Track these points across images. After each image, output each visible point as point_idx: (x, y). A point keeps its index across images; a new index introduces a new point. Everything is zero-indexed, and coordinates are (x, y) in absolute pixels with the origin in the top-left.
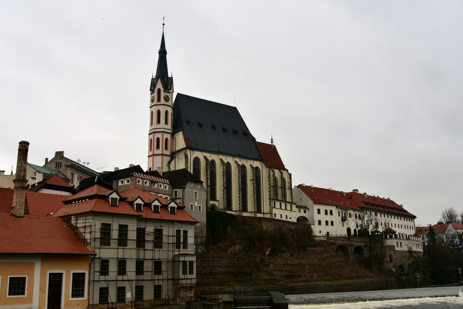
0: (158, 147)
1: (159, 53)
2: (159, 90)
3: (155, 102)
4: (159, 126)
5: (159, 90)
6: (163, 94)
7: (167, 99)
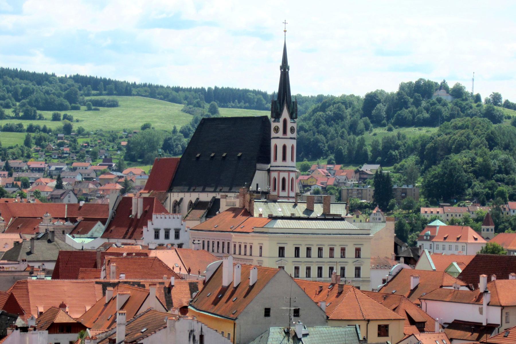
0: (284, 189)
1: (281, 69)
2: (285, 121)
3: (280, 134)
4: (284, 164)
5: (285, 121)
6: (289, 125)
7: (292, 130)
